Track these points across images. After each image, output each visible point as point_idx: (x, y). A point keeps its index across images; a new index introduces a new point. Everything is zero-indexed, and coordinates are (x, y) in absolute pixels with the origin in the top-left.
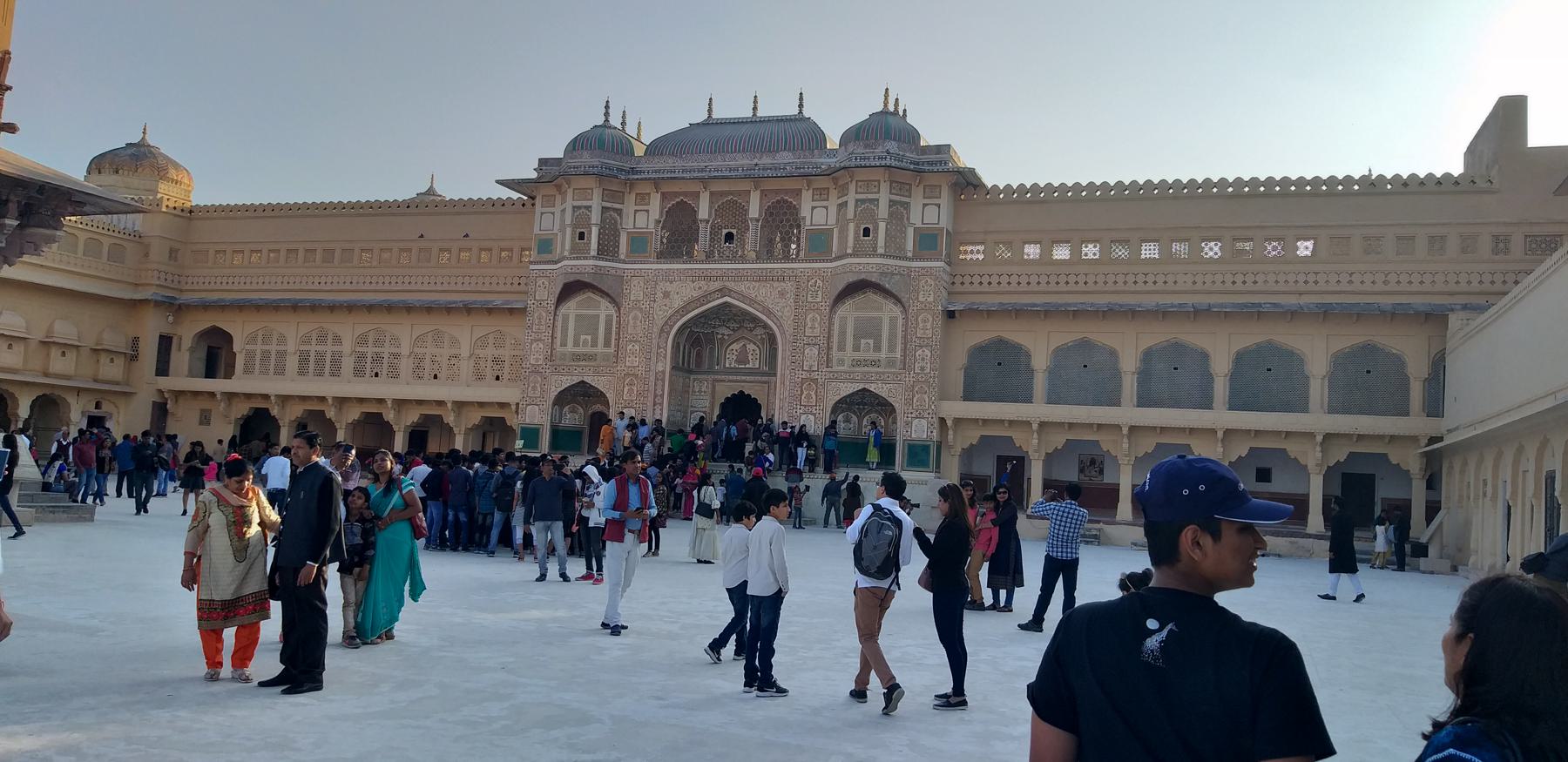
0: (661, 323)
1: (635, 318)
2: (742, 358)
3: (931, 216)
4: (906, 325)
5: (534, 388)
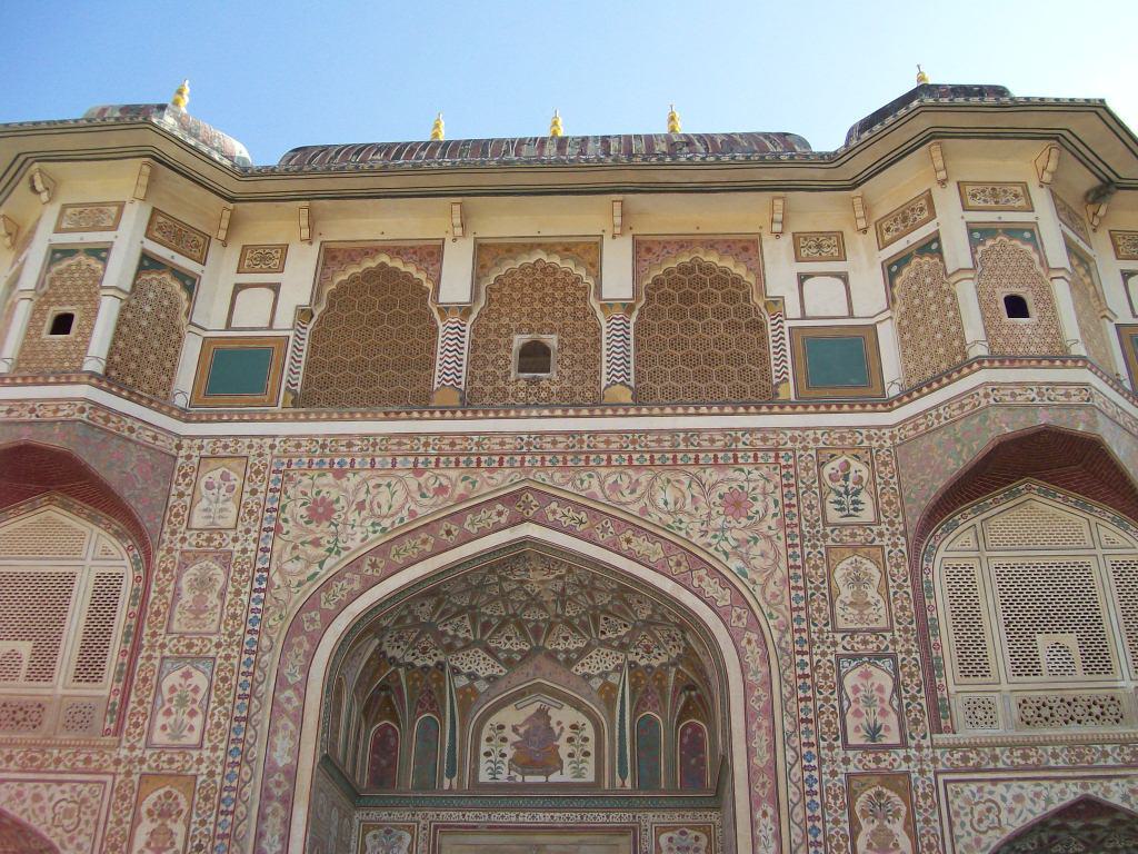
0: (299, 598)
1: (203, 583)
2: (537, 750)
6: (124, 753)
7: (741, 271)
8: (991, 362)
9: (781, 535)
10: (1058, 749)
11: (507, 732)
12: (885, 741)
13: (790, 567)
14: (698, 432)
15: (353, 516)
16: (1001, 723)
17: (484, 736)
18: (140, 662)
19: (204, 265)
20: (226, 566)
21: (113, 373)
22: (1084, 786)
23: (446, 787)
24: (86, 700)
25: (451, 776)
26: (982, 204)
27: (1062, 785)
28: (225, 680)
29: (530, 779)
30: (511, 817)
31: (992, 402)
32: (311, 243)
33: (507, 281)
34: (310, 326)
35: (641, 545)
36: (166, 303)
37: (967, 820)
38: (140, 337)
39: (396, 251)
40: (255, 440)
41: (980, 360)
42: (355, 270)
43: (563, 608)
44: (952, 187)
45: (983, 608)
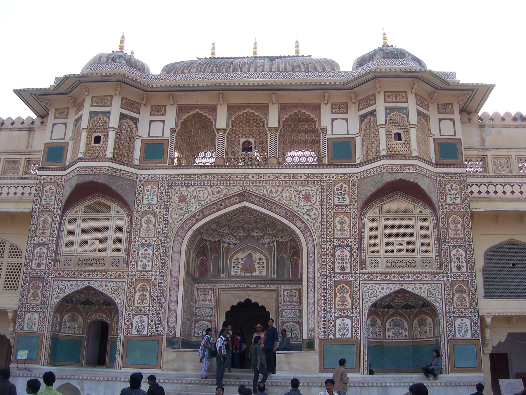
0: (178, 226)
1: (148, 222)
2: (249, 266)
3: (447, 129)
4: (437, 226)
5: (35, 295)
6: (130, 273)
7: (314, 116)
8: (386, 157)
9: (320, 208)
10: (395, 275)
11: (240, 260)
12: (346, 271)
13: (322, 218)
14: (297, 174)
15: (192, 200)
16: (380, 267)
17: (233, 262)
18: (132, 246)
20: (155, 217)
21: (116, 156)
22: (402, 286)
23: (222, 277)
24: (117, 258)
25: (223, 273)
26: (390, 100)
27: (395, 285)
28: (157, 251)
29: (246, 275)
30: (241, 286)
33: (238, 119)
34: (175, 135)
35: (279, 210)
36: (129, 129)
37: (367, 294)
38: (122, 142)
41: (383, 157)
43: (256, 224)
44: (382, 94)
45: (379, 232)
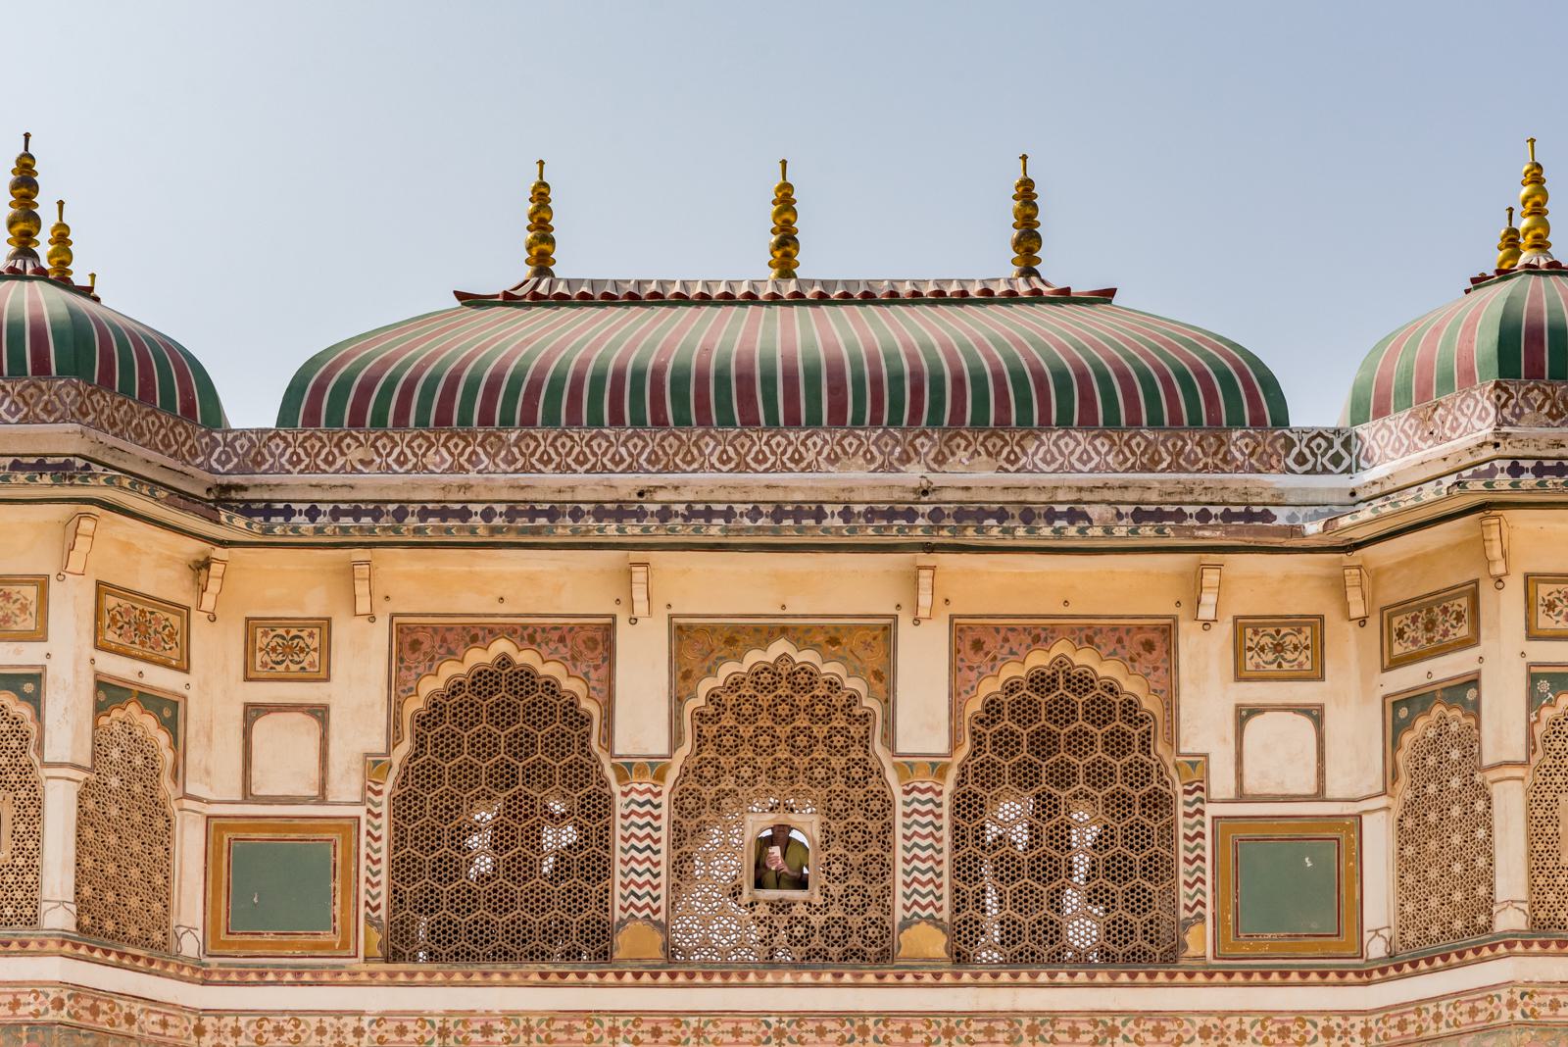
7: (1131, 686)
14: (1054, 1017)
19: (187, 671)
31: (1519, 1017)
32: (372, 618)
33: (730, 699)
34: (388, 787)
36: (138, 761)
38: (113, 839)
39: (529, 635)
40: (328, 1020)
42: (449, 670)
